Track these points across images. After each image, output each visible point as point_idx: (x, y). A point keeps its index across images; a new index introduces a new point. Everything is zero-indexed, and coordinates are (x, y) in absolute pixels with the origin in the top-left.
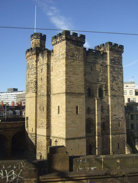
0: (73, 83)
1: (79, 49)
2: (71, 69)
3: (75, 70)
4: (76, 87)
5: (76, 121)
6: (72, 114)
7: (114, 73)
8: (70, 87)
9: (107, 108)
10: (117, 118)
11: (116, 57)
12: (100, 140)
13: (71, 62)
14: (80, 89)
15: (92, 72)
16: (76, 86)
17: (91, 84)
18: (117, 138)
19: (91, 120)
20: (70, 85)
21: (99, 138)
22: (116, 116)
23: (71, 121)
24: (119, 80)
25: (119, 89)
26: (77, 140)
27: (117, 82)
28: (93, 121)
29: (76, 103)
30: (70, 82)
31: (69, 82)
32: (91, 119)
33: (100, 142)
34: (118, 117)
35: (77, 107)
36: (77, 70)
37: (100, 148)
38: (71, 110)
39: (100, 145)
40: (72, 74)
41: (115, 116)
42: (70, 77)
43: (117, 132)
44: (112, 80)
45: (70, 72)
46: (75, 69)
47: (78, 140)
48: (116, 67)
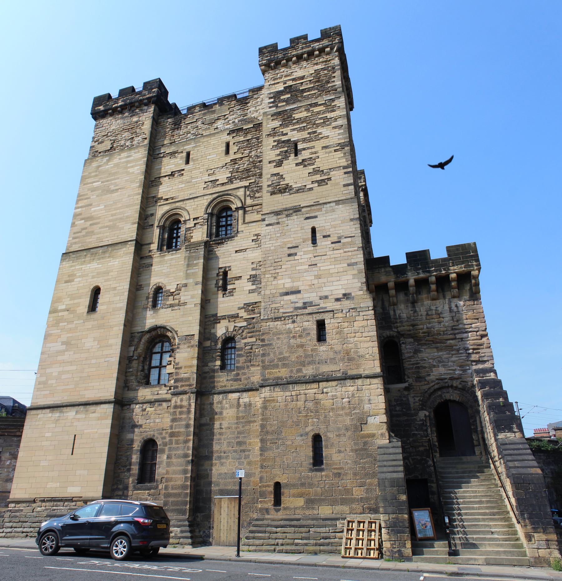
0: (99, 218)
1: (137, 122)
2: (95, 184)
3: (108, 181)
4: (107, 227)
5: (83, 341)
6: (72, 316)
7: (285, 130)
8: (84, 233)
9: (253, 269)
10: (305, 305)
11: (303, 78)
12: (189, 412)
13: (99, 166)
14: (123, 228)
15: (187, 167)
16: (109, 224)
17: (178, 204)
18: (300, 404)
19: (169, 334)
20: (86, 228)
21: (181, 407)
22: (299, 292)
23: (63, 343)
24: (318, 145)
25: (318, 177)
26: (71, 413)
27: (305, 155)
28: (174, 339)
29: (93, 277)
30: (86, 219)
31: (83, 221)
32: (164, 328)
33: (188, 426)
34: (312, 297)
35: (96, 292)
36: (118, 178)
37: (186, 456)
38: (72, 302)
39: (186, 441)
40: (97, 196)
41: (292, 297)
42: (91, 205)
43: (309, 371)
44: (280, 157)
45: (92, 192)
46: (113, 177)
47: (77, 412)
48: (298, 108)
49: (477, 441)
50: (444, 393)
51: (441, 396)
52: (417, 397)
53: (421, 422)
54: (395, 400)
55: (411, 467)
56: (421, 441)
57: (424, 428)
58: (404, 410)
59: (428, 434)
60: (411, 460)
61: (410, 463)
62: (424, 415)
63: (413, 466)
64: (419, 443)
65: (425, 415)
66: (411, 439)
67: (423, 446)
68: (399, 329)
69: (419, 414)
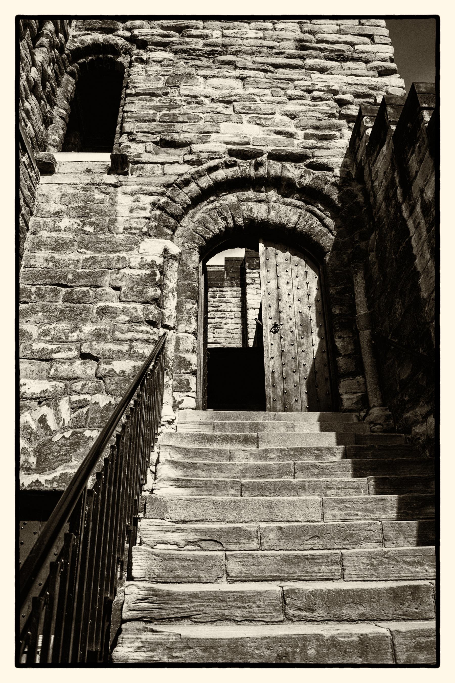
49: (349, 356)
50: (249, 200)
51: (235, 207)
52: (150, 194)
53: (144, 272)
54: (63, 196)
55: (57, 438)
56: (129, 335)
57: (152, 292)
58: (87, 228)
59: (162, 314)
60: (64, 405)
61: (58, 418)
62: (161, 250)
63: (67, 434)
64: (119, 342)
65: (166, 250)
66: (88, 328)
67: (131, 355)
68: (136, 32)
69: (142, 245)
